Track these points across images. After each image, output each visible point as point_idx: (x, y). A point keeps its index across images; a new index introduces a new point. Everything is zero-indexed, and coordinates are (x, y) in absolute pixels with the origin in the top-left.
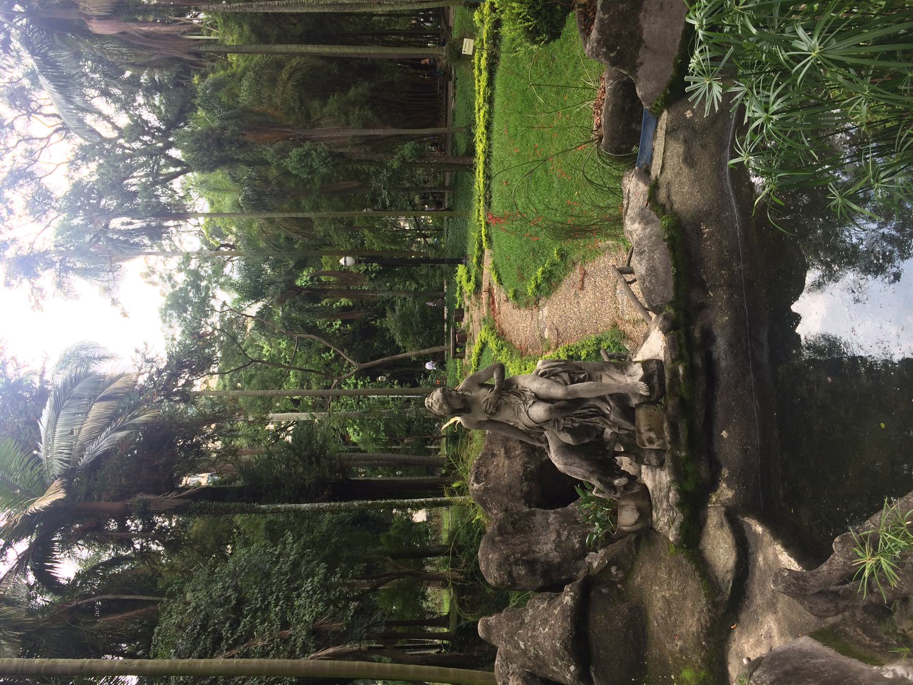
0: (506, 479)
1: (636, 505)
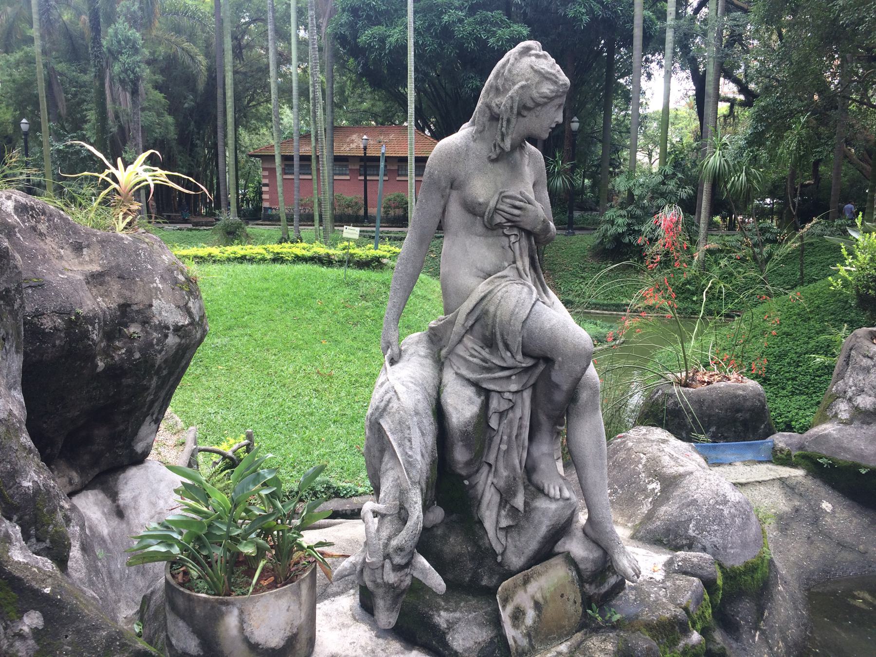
0: (56, 279)
1: (299, 628)
